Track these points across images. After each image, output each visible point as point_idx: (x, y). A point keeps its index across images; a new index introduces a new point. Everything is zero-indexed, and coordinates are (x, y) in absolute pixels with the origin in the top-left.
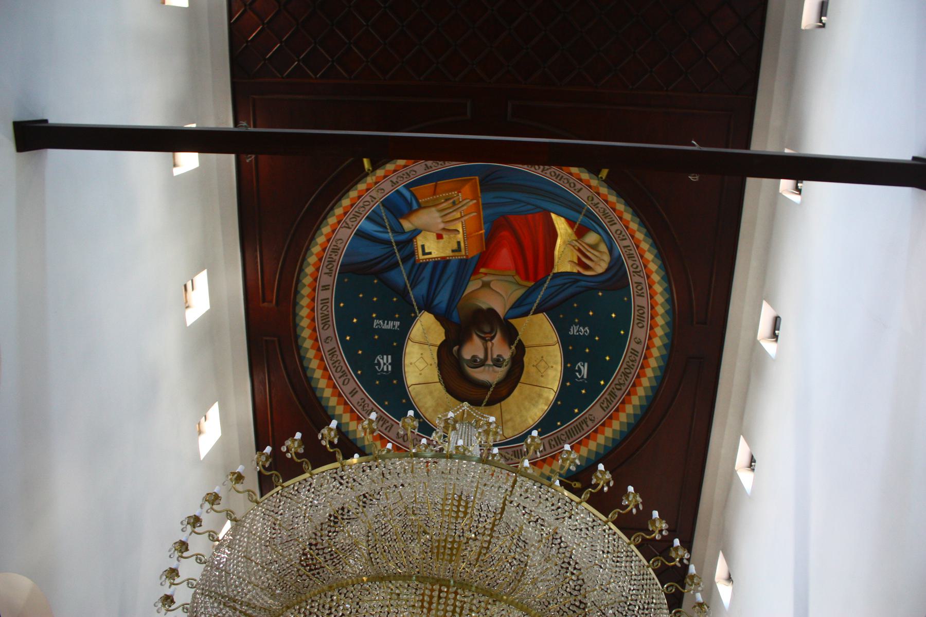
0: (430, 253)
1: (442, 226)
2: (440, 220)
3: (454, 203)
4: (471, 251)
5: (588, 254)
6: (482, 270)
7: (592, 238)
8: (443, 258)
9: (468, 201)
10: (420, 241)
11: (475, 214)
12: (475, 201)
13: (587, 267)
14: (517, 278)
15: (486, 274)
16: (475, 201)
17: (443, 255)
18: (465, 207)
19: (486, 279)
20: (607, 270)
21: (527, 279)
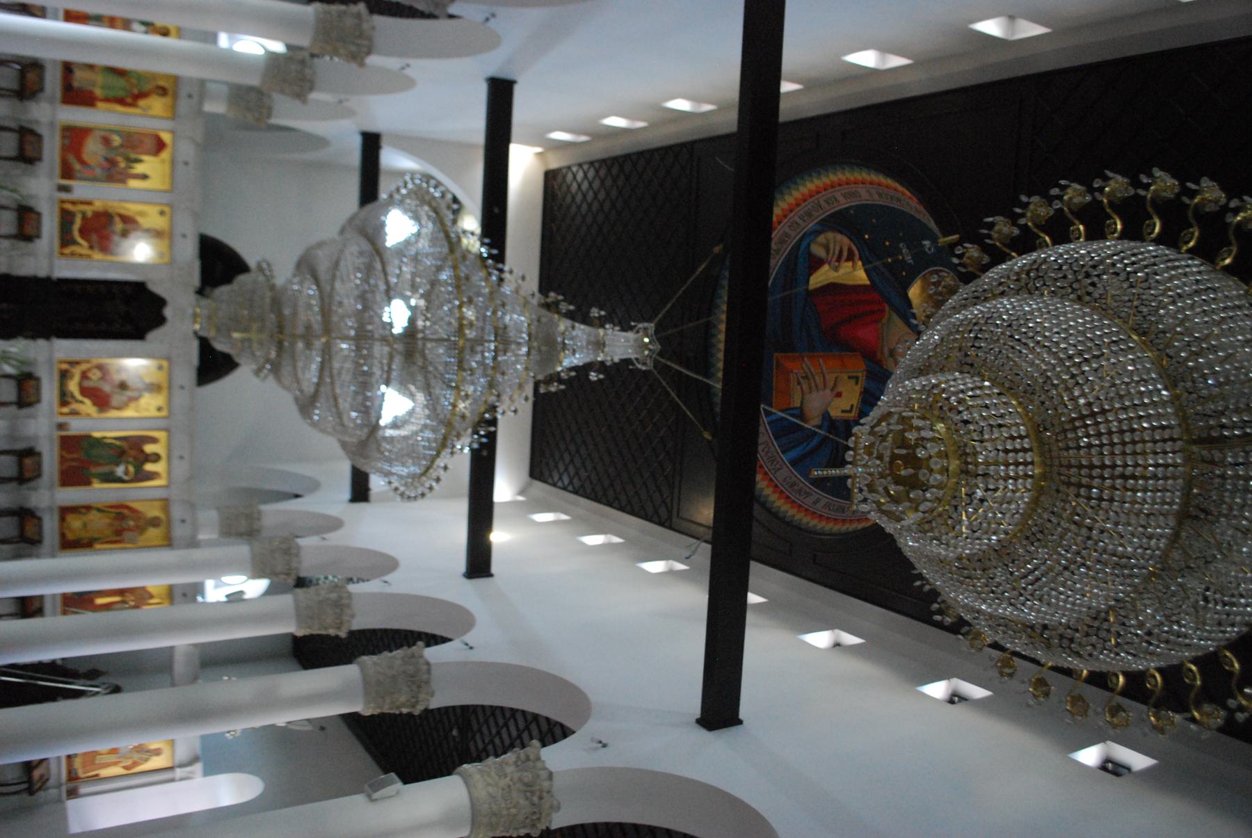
0: (852, 406)
1: (828, 391)
2: (821, 393)
3: (806, 377)
4: (859, 367)
5: (837, 252)
6: (879, 355)
7: (817, 250)
8: (861, 393)
9: (804, 365)
10: (835, 413)
11: (821, 360)
12: (806, 359)
13: (850, 251)
14: (884, 321)
15: (882, 353)
16: (806, 359)
17: (858, 394)
18: (812, 370)
19: (886, 351)
20: (841, 233)
21: (883, 311)
